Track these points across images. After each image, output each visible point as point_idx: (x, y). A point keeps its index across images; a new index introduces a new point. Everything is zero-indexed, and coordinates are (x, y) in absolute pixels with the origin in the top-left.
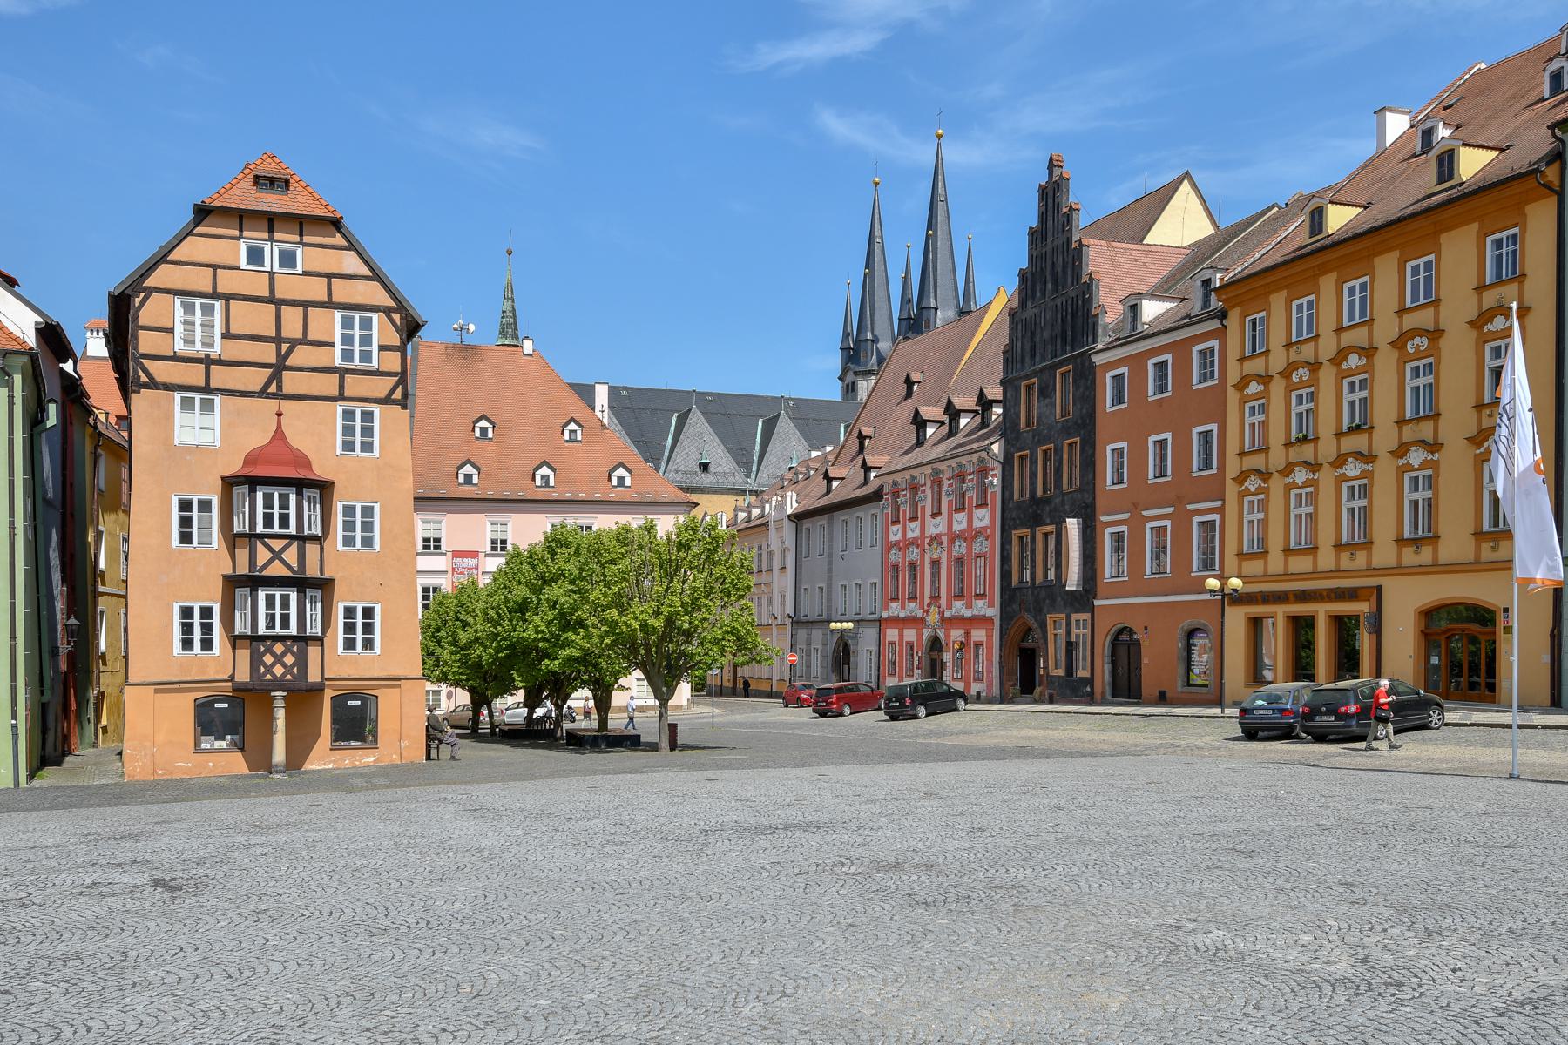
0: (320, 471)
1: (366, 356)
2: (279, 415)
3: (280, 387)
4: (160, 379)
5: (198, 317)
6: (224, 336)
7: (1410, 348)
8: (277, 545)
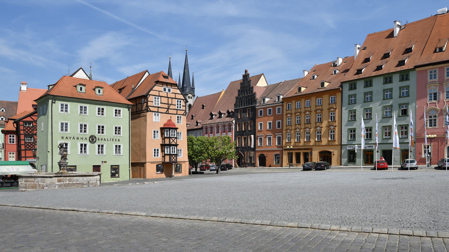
0: (177, 126)
1: (180, 107)
2: (171, 117)
3: (168, 112)
4: (151, 110)
5: (157, 100)
7: (317, 112)
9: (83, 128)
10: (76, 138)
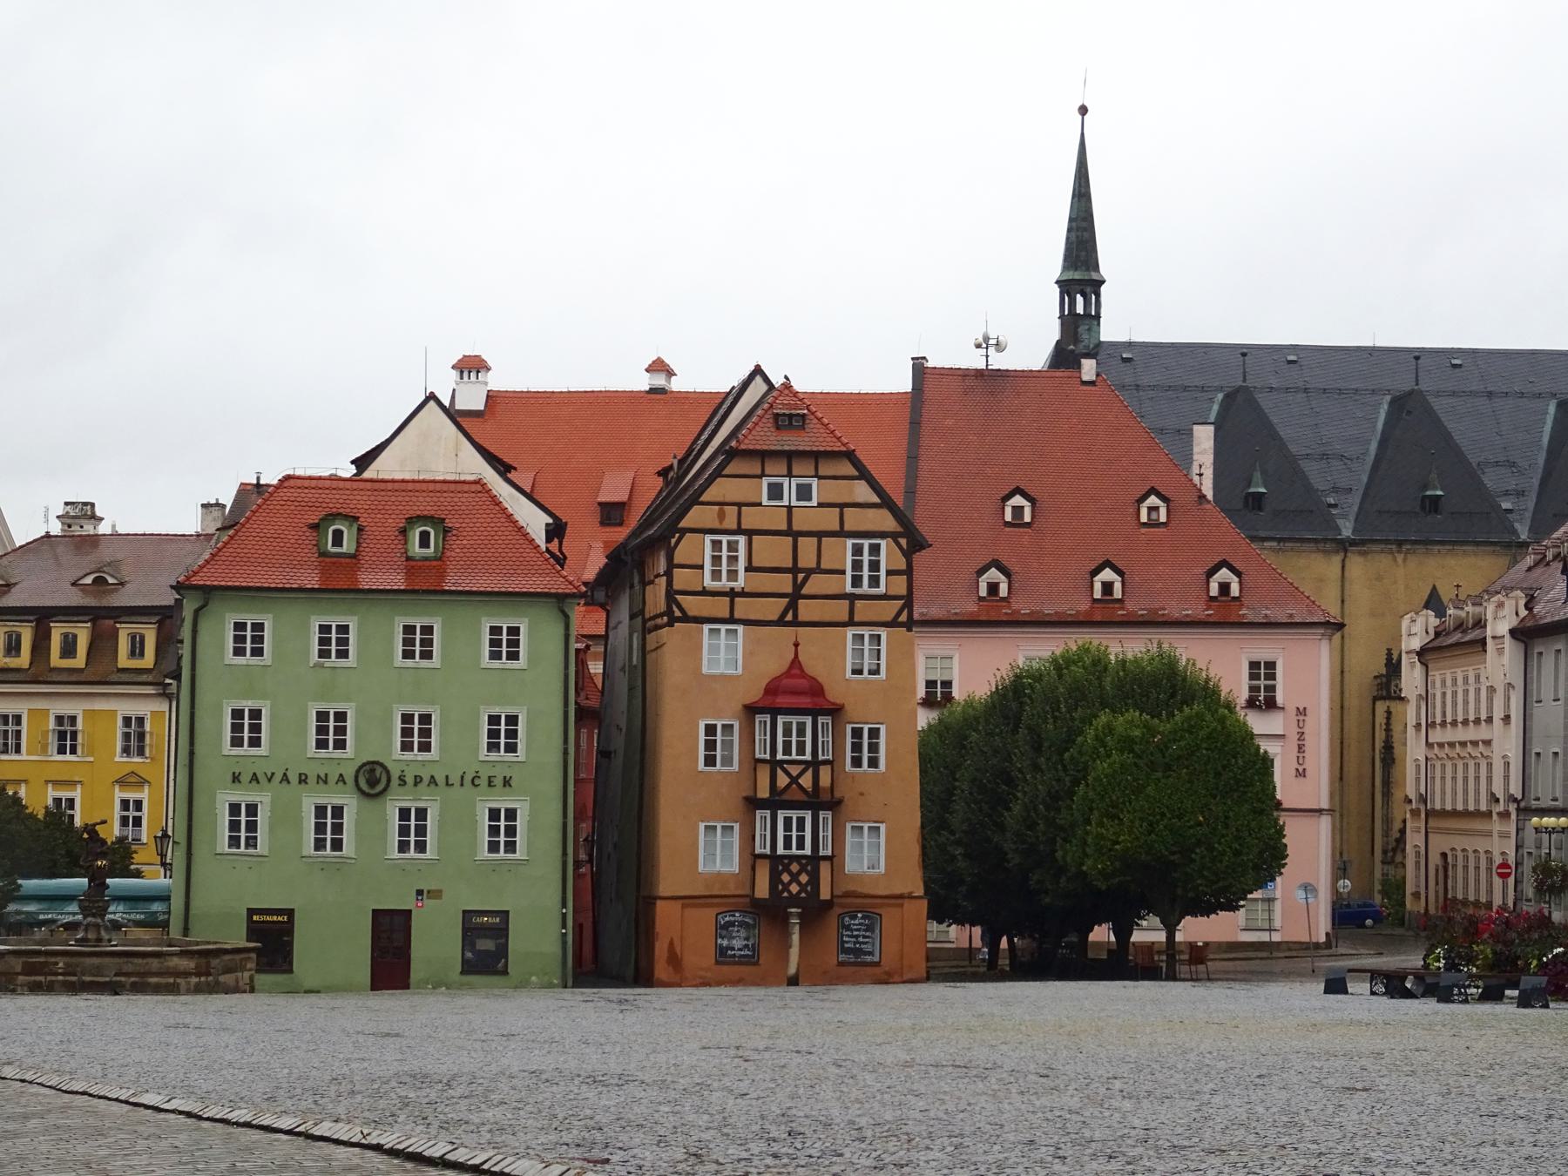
0: (834, 694)
1: (874, 581)
2: (796, 645)
3: (795, 615)
4: (690, 613)
6: (747, 570)
8: (795, 770)
9: (331, 729)
10: (294, 778)
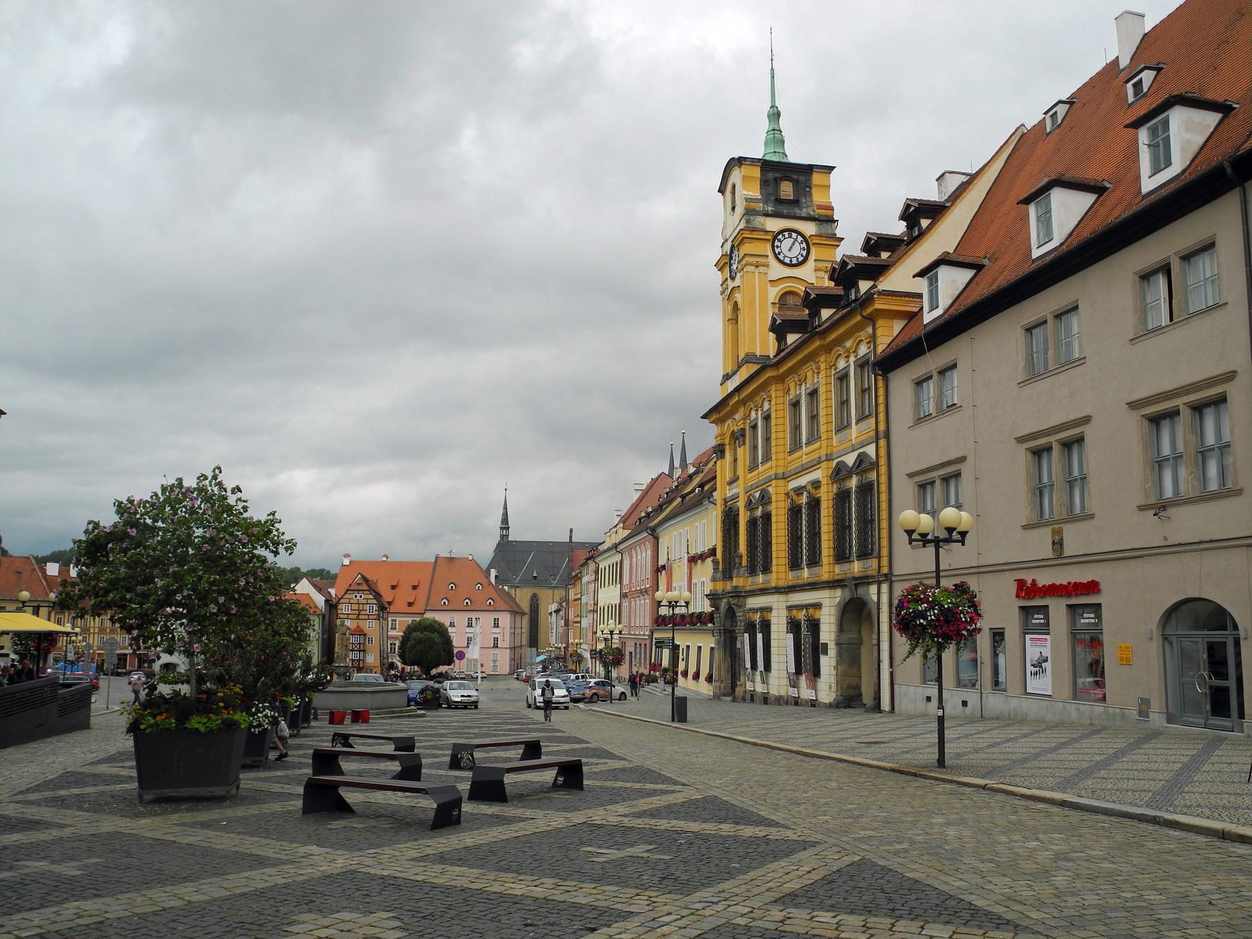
0: (365, 632)
